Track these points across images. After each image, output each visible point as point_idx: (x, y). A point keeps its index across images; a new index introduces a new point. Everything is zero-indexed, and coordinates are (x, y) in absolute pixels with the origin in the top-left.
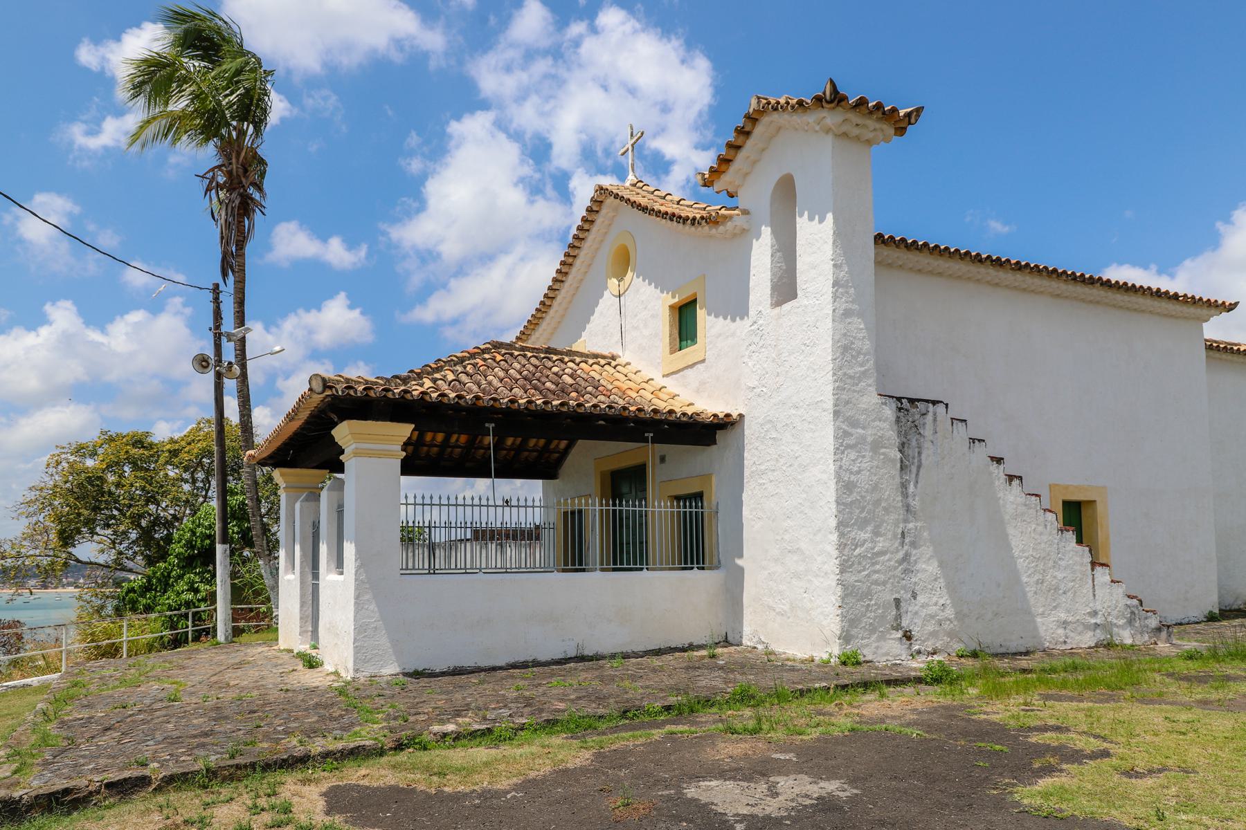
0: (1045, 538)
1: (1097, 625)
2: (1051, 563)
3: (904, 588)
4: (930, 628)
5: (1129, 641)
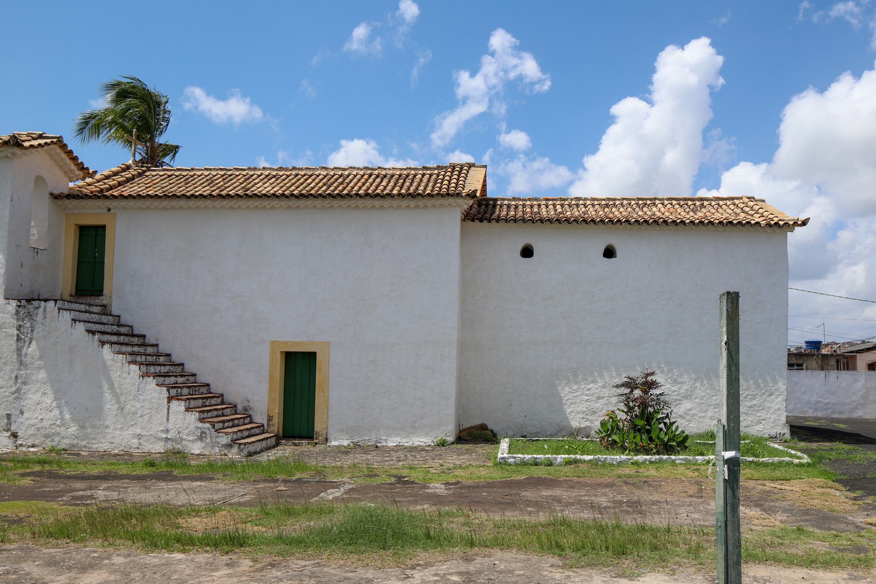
0: (128, 381)
1: (167, 439)
2: (131, 397)
3: (15, 408)
4: (31, 432)
5: (197, 452)
